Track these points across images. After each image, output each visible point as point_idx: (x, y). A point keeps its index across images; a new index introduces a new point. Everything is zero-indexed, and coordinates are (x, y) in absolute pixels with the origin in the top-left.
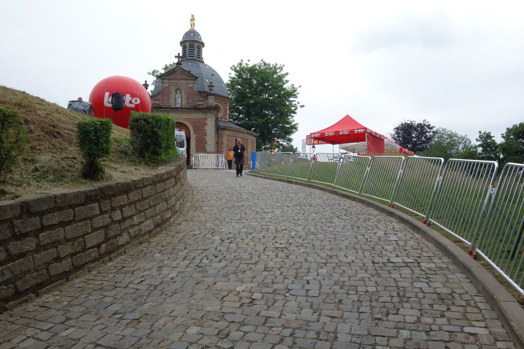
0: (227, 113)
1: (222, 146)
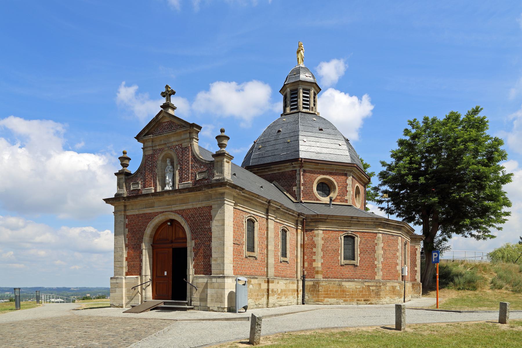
0: (347, 191)
1: (314, 250)
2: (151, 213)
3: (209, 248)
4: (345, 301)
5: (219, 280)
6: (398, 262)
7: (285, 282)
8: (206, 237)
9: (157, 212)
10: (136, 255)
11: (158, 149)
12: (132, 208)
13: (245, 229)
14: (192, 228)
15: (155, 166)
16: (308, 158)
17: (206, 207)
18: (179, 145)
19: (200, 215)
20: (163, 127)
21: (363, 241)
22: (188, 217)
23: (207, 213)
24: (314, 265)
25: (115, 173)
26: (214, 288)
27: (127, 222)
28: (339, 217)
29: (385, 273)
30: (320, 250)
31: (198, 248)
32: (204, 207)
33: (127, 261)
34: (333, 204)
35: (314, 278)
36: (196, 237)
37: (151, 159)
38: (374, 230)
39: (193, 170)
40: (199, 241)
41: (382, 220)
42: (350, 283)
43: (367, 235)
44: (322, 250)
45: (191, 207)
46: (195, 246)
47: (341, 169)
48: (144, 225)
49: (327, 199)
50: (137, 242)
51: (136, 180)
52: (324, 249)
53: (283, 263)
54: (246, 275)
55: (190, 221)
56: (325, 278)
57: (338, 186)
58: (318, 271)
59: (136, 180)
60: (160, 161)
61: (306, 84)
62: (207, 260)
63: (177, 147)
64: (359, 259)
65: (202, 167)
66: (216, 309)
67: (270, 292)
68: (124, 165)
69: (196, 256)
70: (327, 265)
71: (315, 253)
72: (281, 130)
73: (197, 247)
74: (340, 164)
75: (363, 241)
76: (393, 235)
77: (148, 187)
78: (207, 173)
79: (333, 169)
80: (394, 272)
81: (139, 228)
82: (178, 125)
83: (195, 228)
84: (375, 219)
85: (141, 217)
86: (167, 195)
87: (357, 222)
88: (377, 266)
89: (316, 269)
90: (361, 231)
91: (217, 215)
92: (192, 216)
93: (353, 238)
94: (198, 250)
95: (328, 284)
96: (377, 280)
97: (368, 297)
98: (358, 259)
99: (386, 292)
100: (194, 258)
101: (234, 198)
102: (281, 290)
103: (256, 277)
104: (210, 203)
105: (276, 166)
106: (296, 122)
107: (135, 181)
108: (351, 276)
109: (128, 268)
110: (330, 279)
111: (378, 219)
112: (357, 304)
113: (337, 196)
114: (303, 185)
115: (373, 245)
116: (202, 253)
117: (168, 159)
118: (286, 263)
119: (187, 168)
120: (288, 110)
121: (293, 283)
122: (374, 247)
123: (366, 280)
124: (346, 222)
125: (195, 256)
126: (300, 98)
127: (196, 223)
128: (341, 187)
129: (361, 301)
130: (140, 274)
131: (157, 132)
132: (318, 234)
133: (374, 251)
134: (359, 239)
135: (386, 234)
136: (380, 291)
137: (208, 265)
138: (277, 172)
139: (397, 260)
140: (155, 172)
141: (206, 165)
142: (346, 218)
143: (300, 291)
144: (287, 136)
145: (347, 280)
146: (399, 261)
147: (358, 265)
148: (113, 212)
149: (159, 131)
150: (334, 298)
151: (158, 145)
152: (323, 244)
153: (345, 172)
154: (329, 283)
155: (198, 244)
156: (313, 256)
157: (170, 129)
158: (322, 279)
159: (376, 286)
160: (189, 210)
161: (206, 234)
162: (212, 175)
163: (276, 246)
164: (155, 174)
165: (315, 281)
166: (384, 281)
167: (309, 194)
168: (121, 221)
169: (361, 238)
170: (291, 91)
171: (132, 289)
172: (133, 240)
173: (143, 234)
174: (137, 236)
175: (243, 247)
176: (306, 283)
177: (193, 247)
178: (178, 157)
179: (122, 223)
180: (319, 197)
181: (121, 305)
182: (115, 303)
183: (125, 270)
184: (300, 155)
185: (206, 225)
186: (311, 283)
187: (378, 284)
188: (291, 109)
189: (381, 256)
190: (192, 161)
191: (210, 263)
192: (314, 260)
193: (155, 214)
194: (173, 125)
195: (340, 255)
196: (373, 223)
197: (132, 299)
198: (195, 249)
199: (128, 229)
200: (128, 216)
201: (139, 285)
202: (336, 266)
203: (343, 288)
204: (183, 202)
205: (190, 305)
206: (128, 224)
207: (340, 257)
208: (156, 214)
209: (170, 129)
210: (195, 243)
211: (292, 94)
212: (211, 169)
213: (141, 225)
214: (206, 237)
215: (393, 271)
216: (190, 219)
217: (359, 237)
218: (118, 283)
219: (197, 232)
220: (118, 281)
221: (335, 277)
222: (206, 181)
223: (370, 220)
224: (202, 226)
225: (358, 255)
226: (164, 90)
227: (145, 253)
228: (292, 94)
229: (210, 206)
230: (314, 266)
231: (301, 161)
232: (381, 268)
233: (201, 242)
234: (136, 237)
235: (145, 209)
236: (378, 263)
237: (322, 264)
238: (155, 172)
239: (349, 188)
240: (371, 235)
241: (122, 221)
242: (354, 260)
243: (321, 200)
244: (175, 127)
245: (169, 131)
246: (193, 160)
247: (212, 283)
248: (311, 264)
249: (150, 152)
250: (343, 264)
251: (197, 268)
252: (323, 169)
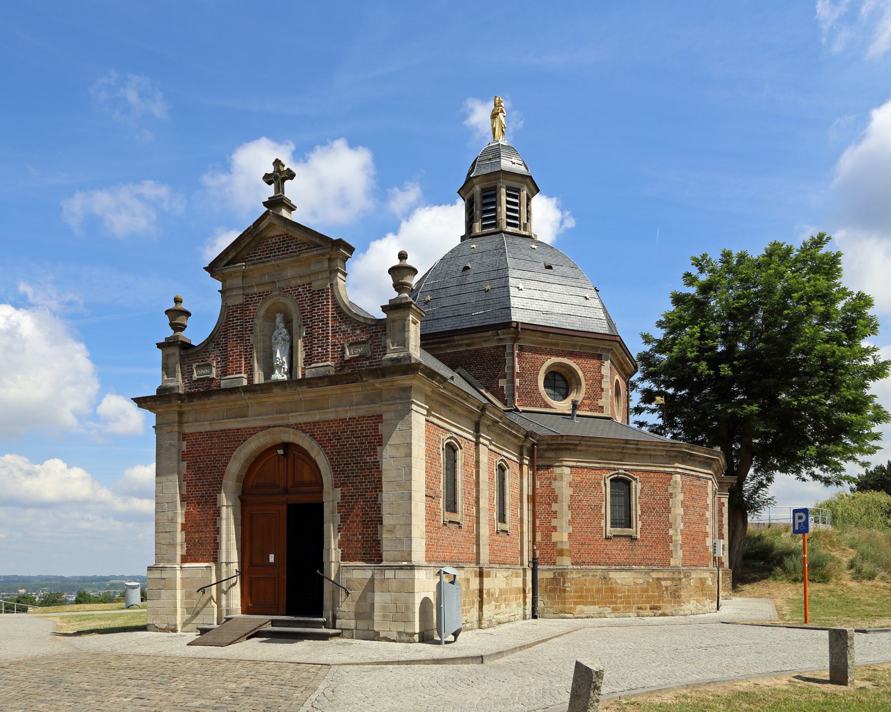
0: (602, 390)
1: (555, 507)
2: (241, 429)
3: (376, 504)
4: (615, 610)
5: (401, 574)
7: (505, 573)
8: (368, 482)
9: (255, 428)
10: (204, 520)
11: (256, 294)
12: (196, 418)
13: (442, 465)
14: (335, 462)
15: (249, 328)
16: (527, 322)
17: (368, 417)
18: (304, 285)
19: (352, 435)
20: (268, 248)
21: (646, 489)
22: (325, 437)
23: (369, 430)
24: (555, 537)
25: (157, 344)
26: (389, 592)
27: (184, 449)
29: (687, 554)
30: (566, 508)
31: (349, 505)
32: (364, 417)
33: (184, 532)
34: (578, 416)
35: (554, 564)
36: (343, 480)
37: (240, 313)
39: (337, 339)
40: (351, 490)
42: (624, 575)
43: (654, 476)
44: (570, 508)
45: (332, 416)
46: (341, 500)
48: (223, 454)
49: (565, 405)
50: (209, 490)
51: (204, 358)
52: (574, 505)
53: (501, 534)
54: (444, 561)
55: (331, 446)
56: (576, 564)
57: (586, 380)
58: (562, 549)
59: (204, 358)
60: (261, 319)
61: (513, 178)
62: (371, 531)
63: (301, 290)
64: (640, 524)
65: (358, 332)
66: (394, 636)
67: (485, 596)
68: (178, 327)
69: (345, 522)
70: (579, 538)
71: (556, 512)
72: (469, 265)
73: (346, 502)
74: (590, 336)
75: (646, 489)
76: (699, 477)
77: (233, 374)
78: (369, 345)
79: (575, 346)
80: (702, 550)
81: (212, 461)
82: (302, 244)
83: (343, 461)
84: (669, 445)
85: (216, 437)
86: (279, 390)
88: (674, 538)
89: (559, 546)
90: (643, 468)
91: (394, 435)
92: (334, 437)
93: (628, 483)
94: (350, 509)
95: (583, 576)
96: (673, 567)
97: (658, 601)
98: (638, 524)
100: (340, 525)
101: (428, 399)
102: (500, 590)
103: (461, 565)
104: (375, 409)
105: (464, 337)
106: (501, 251)
107: (202, 361)
108: (625, 559)
109: (187, 547)
110: (586, 565)
112: (638, 616)
113: (583, 399)
114: (520, 375)
115: (665, 498)
116: (357, 516)
117: (278, 314)
118: (505, 534)
119: (323, 334)
120: (477, 228)
121: (517, 576)
122: (668, 500)
123: (654, 568)
124: (615, 451)
125: (341, 522)
126: (501, 205)
127: (344, 451)
128: (591, 381)
129: (645, 609)
130: (216, 560)
131: (255, 256)
132: (561, 476)
133: (667, 508)
134: (639, 486)
135: (688, 475)
136: (681, 589)
137: (373, 540)
138: (465, 348)
139: (707, 527)
140: (249, 343)
141: (366, 327)
142: (616, 443)
143: (529, 592)
144: (482, 277)
145: (617, 568)
146: (709, 529)
147: (639, 537)
148: (153, 427)
149: (259, 256)
150: (594, 604)
151: (256, 285)
152: (571, 496)
153: (599, 352)
154: (584, 574)
155: (350, 496)
156: (553, 520)
157: (284, 251)
158: (571, 567)
159: (673, 579)
160: (329, 424)
161: (369, 475)
162: (381, 349)
163: (491, 499)
164: (248, 346)
165: (558, 571)
166: (686, 568)
167: (531, 395)
168: (171, 445)
169: (642, 484)
170: (483, 190)
171: (198, 591)
172: (198, 485)
173: (222, 474)
174: (207, 479)
175: (439, 503)
176: (540, 575)
177: (338, 503)
178: (302, 310)
179: (175, 450)
180: (549, 400)
181: (173, 627)
182: (158, 622)
183: (180, 551)
184: (512, 317)
185: (367, 456)
186: (550, 575)
187: (676, 576)
188: (484, 227)
189: (679, 519)
190: (335, 320)
191: (378, 537)
192: (555, 528)
193: (250, 431)
194: (292, 242)
195: (604, 518)
196: (664, 453)
197: (198, 614)
198: (341, 506)
199: (187, 463)
200: (187, 434)
201: (212, 583)
202: (596, 540)
203: (611, 584)
204: (313, 405)
205: (331, 626)
206: (187, 451)
207: (603, 521)
208: (253, 431)
209: (284, 251)
210: (341, 493)
211: (484, 197)
212: (377, 335)
213: (216, 455)
214: (368, 482)
215: (700, 548)
216: (329, 443)
217: (640, 482)
218: (164, 579)
219: (346, 470)
220: (165, 575)
221: (594, 563)
222: (367, 362)
223: (660, 448)
224: (358, 457)
225: (638, 517)
226: (271, 170)
227: (227, 513)
228: (484, 197)
229: (377, 416)
230: (554, 539)
231: (517, 327)
232: (680, 542)
233: (357, 492)
234: (205, 479)
235: (226, 420)
236: (675, 533)
237: (570, 535)
238: (249, 343)
239: (606, 385)
240: (662, 478)
241: (173, 445)
242: (630, 528)
243: (553, 406)
244: (296, 248)
245: (282, 254)
246: (336, 317)
247: (383, 580)
248: (547, 536)
249: (239, 300)
250: (610, 535)
251: (347, 547)
252: (557, 345)
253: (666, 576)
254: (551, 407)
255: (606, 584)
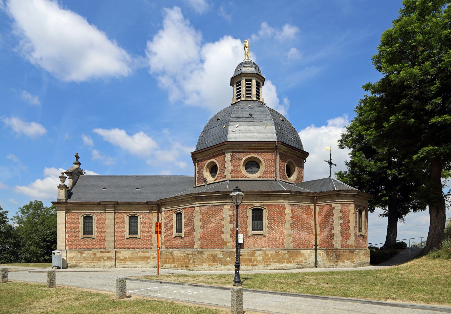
4: (175, 266)
6: (223, 231)
28: (168, 199)
38: (193, 205)
41: (193, 195)
47: (219, 149)
74: (218, 146)
79: (214, 153)
84: (188, 195)
87: (182, 201)
90: (182, 207)
96: (195, 249)
98: (183, 231)
99: (202, 260)
111: (191, 195)
112: (182, 270)
129: (184, 267)
135: (206, 206)
139: (222, 229)
147: (184, 236)
150: (168, 263)
159: (193, 254)
187: (194, 253)
232: (199, 238)
252: (208, 155)
253: (190, 253)
254: (246, 177)
255: (172, 256)
